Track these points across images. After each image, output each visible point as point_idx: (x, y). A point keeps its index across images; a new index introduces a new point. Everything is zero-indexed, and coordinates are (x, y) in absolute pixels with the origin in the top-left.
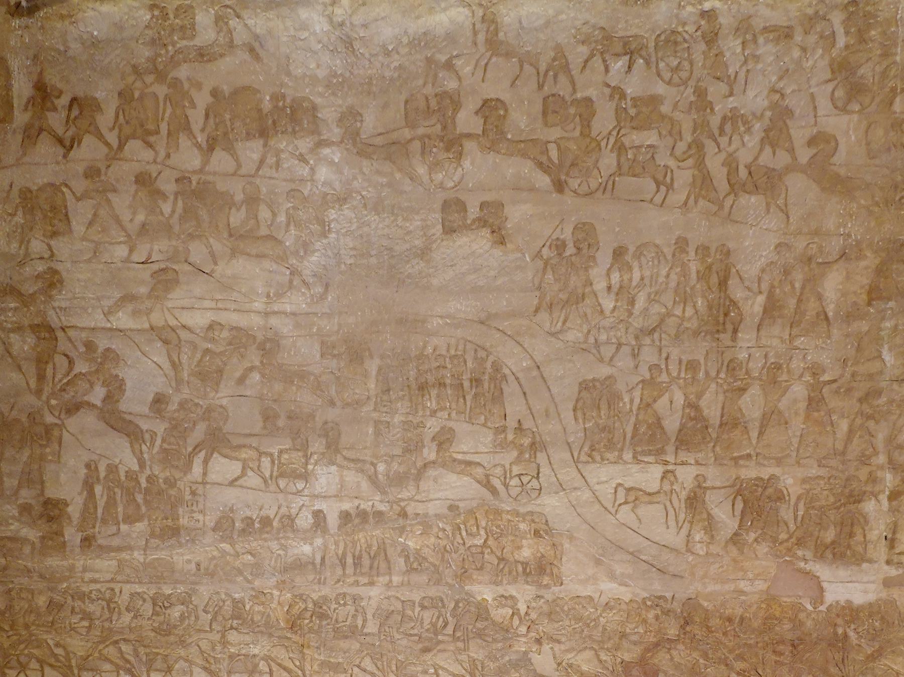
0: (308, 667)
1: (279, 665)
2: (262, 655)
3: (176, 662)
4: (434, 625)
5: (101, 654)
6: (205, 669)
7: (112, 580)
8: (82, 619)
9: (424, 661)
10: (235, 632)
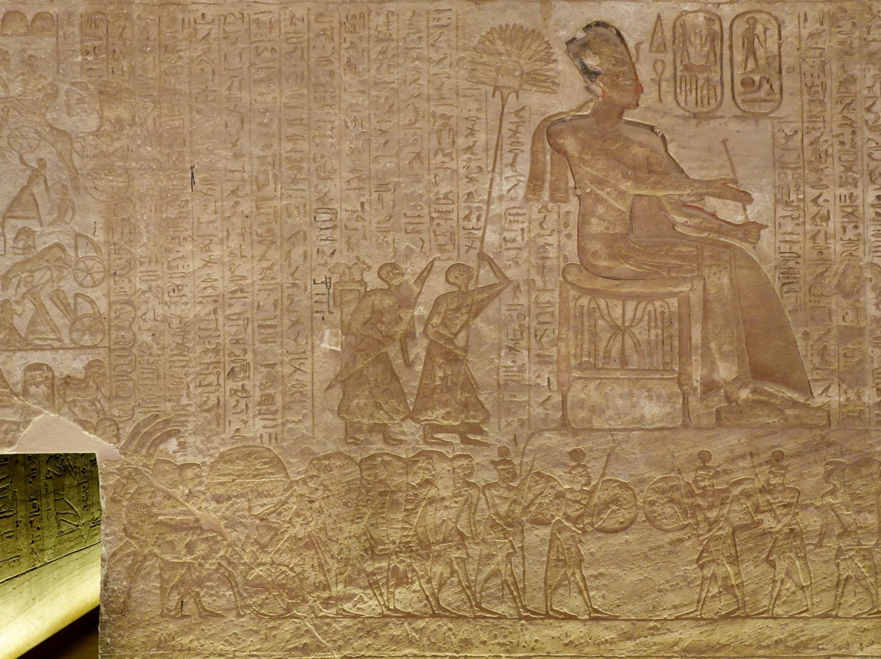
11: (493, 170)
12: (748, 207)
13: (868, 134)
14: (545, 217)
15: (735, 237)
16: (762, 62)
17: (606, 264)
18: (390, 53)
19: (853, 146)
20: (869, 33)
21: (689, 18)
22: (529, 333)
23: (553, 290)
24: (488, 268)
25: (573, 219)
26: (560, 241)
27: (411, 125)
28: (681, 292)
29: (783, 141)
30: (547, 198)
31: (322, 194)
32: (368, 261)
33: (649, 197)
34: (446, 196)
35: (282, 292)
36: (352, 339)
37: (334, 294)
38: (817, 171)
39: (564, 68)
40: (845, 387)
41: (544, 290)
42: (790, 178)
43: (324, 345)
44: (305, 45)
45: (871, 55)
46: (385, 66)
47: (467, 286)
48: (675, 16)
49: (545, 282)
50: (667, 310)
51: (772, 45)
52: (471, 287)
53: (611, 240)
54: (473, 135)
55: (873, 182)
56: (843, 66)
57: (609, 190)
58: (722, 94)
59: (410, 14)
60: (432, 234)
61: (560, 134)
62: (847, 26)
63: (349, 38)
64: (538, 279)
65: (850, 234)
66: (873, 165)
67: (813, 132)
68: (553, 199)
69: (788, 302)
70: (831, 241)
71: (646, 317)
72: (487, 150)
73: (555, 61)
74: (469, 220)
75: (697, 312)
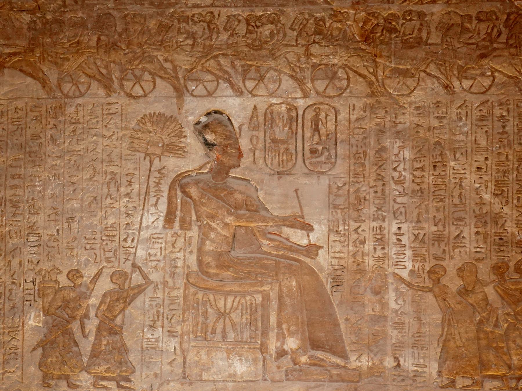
0: (380, 73)
1: (355, 72)
2: (340, 64)
3: (267, 72)
4: (489, 34)
5: (203, 67)
6: (292, 77)
7: (212, 5)
8: (186, 38)
9: (482, 65)
10: (317, 46)
11: (143, 209)
12: (310, 234)
13: (393, 186)
14: (176, 240)
15: (302, 253)
16: (324, 138)
17: (214, 271)
18: (78, 132)
19: (383, 193)
20: (396, 118)
21: (276, 108)
22: (163, 317)
23: (179, 288)
24: (138, 273)
25: (195, 241)
26: (185, 256)
27: (91, 179)
28: (264, 290)
29: (336, 190)
30: (177, 228)
31: (31, 224)
32: (60, 268)
33: (246, 227)
34: (112, 226)
35: (5, 287)
36: (50, 319)
37: (38, 290)
38: (358, 210)
39: (192, 141)
40: (373, 356)
41: (173, 288)
42: (339, 215)
43: (30, 323)
44: (24, 126)
45: (398, 132)
46: (75, 140)
47: (124, 285)
48: (266, 107)
49: (174, 283)
50: (254, 302)
51: (331, 126)
52: (126, 286)
53: (219, 256)
54: (130, 185)
55: (396, 218)
56: (378, 140)
57: (218, 222)
58: (296, 158)
59: (91, 106)
60: (102, 251)
61: (187, 185)
62: (382, 113)
63: (52, 122)
64: (170, 281)
65: (379, 253)
66: (396, 206)
67: (356, 184)
68: (181, 228)
69: (335, 298)
70: (366, 258)
71: (240, 307)
72: (139, 195)
73: (185, 137)
74: (127, 242)
75: (274, 304)
